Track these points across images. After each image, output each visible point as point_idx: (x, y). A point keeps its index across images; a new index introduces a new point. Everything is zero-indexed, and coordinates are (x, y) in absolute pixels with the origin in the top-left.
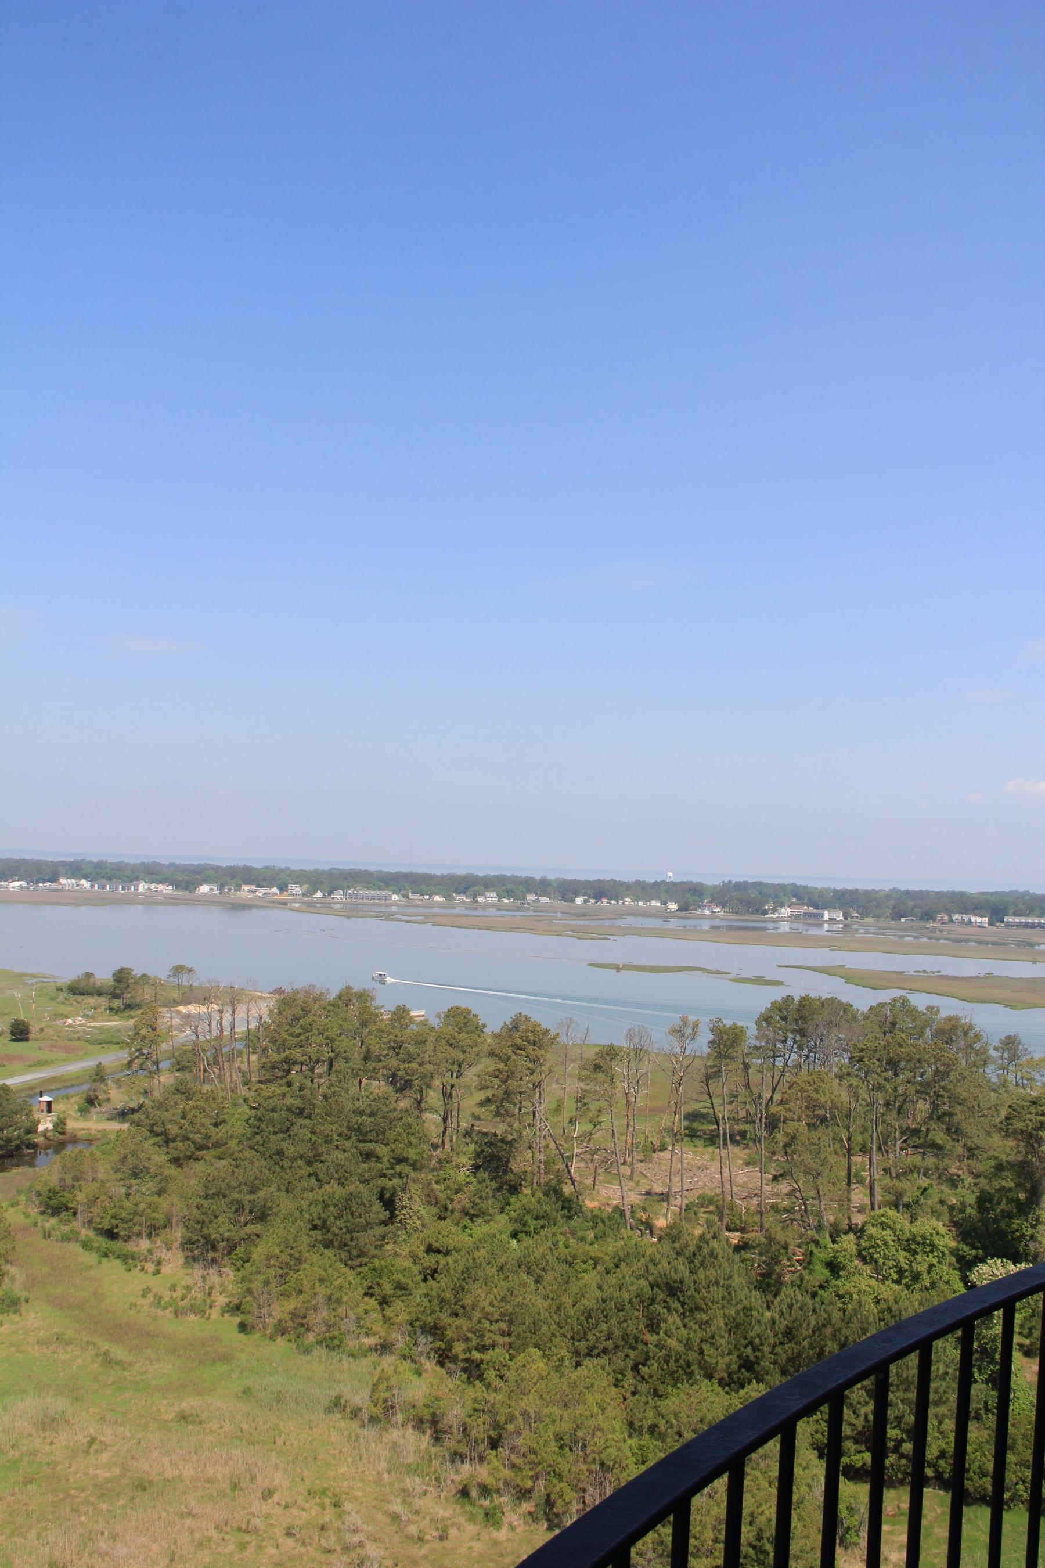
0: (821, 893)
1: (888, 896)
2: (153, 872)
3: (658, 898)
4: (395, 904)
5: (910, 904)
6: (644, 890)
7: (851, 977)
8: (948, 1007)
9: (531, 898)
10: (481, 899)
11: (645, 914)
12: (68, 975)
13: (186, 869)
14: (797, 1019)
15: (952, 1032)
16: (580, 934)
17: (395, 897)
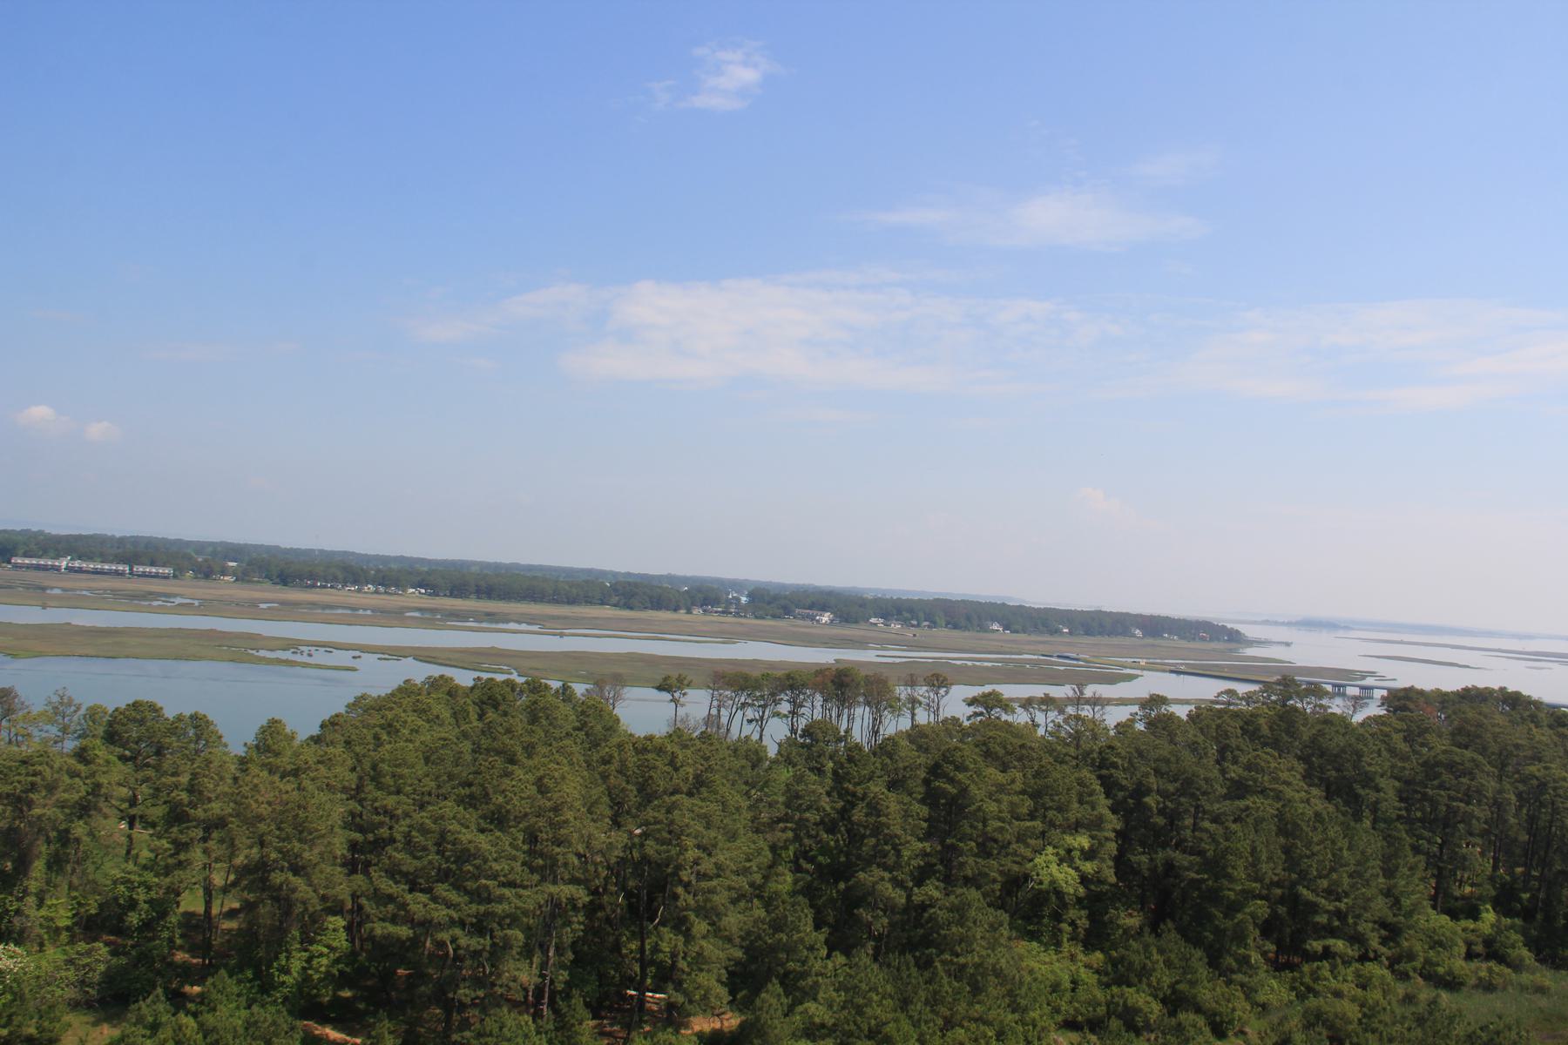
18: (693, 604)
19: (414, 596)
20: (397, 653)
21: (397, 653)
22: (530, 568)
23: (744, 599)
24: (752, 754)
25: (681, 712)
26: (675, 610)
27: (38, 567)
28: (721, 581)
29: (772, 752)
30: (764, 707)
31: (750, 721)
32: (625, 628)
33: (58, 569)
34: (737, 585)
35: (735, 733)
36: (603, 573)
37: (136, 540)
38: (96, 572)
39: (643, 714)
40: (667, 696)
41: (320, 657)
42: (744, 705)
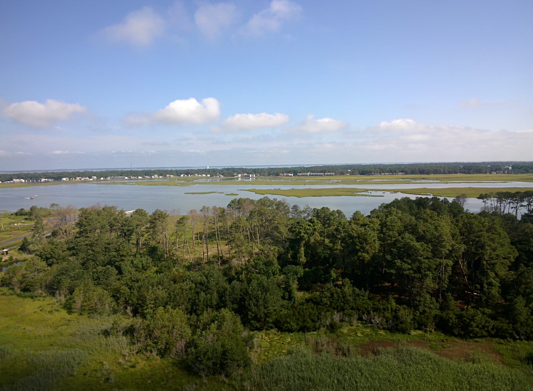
0: (249, 170)
1: (267, 170)
2: (47, 175)
3: (204, 174)
4: (126, 180)
5: (273, 171)
6: (200, 172)
7: (257, 192)
8: (279, 198)
9: (168, 176)
10: (153, 177)
11: (201, 178)
12: (15, 211)
13: (57, 174)
14: (237, 204)
15: (280, 205)
16: (182, 185)
17: (126, 178)
18: (492, 171)
19: (400, 175)
20: (395, 191)
21: (395, 191)
22: (436, 164)
23: (510, 168)
24: (509, 219)
25: (486, 205)
26: (486, 173)
27: (303, 175)
28: (502, 163)
29: (519, 218)
30: (517, 203)
31: (512, 208)
32: (468, 180)
33: (307, 175)
34: (508, 163)
35: (506, 212)
36: (460, 163)
37: (325, 167)
38: (316, 175)
39: (473, 206)
40: (482, 200)
41: (374, 193)
42: (509, 202)
